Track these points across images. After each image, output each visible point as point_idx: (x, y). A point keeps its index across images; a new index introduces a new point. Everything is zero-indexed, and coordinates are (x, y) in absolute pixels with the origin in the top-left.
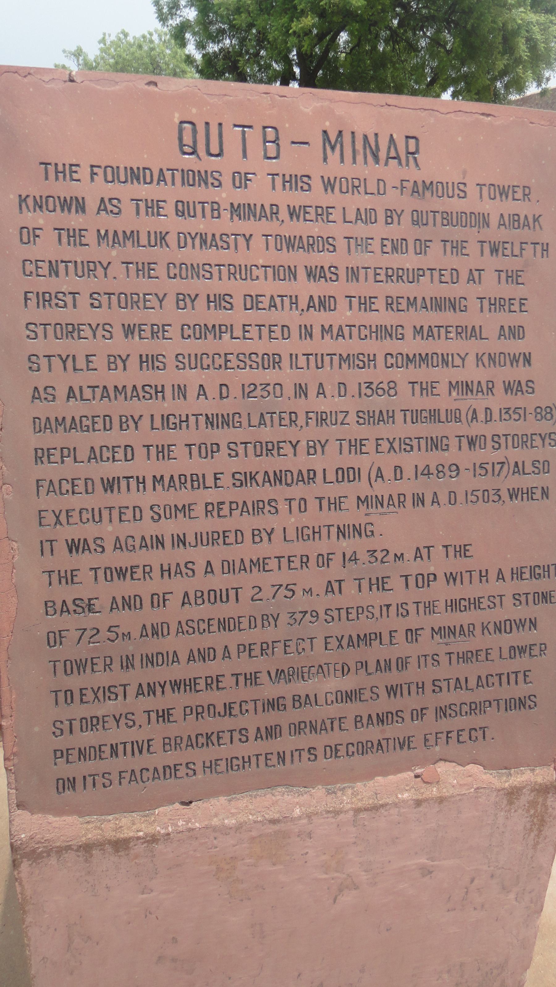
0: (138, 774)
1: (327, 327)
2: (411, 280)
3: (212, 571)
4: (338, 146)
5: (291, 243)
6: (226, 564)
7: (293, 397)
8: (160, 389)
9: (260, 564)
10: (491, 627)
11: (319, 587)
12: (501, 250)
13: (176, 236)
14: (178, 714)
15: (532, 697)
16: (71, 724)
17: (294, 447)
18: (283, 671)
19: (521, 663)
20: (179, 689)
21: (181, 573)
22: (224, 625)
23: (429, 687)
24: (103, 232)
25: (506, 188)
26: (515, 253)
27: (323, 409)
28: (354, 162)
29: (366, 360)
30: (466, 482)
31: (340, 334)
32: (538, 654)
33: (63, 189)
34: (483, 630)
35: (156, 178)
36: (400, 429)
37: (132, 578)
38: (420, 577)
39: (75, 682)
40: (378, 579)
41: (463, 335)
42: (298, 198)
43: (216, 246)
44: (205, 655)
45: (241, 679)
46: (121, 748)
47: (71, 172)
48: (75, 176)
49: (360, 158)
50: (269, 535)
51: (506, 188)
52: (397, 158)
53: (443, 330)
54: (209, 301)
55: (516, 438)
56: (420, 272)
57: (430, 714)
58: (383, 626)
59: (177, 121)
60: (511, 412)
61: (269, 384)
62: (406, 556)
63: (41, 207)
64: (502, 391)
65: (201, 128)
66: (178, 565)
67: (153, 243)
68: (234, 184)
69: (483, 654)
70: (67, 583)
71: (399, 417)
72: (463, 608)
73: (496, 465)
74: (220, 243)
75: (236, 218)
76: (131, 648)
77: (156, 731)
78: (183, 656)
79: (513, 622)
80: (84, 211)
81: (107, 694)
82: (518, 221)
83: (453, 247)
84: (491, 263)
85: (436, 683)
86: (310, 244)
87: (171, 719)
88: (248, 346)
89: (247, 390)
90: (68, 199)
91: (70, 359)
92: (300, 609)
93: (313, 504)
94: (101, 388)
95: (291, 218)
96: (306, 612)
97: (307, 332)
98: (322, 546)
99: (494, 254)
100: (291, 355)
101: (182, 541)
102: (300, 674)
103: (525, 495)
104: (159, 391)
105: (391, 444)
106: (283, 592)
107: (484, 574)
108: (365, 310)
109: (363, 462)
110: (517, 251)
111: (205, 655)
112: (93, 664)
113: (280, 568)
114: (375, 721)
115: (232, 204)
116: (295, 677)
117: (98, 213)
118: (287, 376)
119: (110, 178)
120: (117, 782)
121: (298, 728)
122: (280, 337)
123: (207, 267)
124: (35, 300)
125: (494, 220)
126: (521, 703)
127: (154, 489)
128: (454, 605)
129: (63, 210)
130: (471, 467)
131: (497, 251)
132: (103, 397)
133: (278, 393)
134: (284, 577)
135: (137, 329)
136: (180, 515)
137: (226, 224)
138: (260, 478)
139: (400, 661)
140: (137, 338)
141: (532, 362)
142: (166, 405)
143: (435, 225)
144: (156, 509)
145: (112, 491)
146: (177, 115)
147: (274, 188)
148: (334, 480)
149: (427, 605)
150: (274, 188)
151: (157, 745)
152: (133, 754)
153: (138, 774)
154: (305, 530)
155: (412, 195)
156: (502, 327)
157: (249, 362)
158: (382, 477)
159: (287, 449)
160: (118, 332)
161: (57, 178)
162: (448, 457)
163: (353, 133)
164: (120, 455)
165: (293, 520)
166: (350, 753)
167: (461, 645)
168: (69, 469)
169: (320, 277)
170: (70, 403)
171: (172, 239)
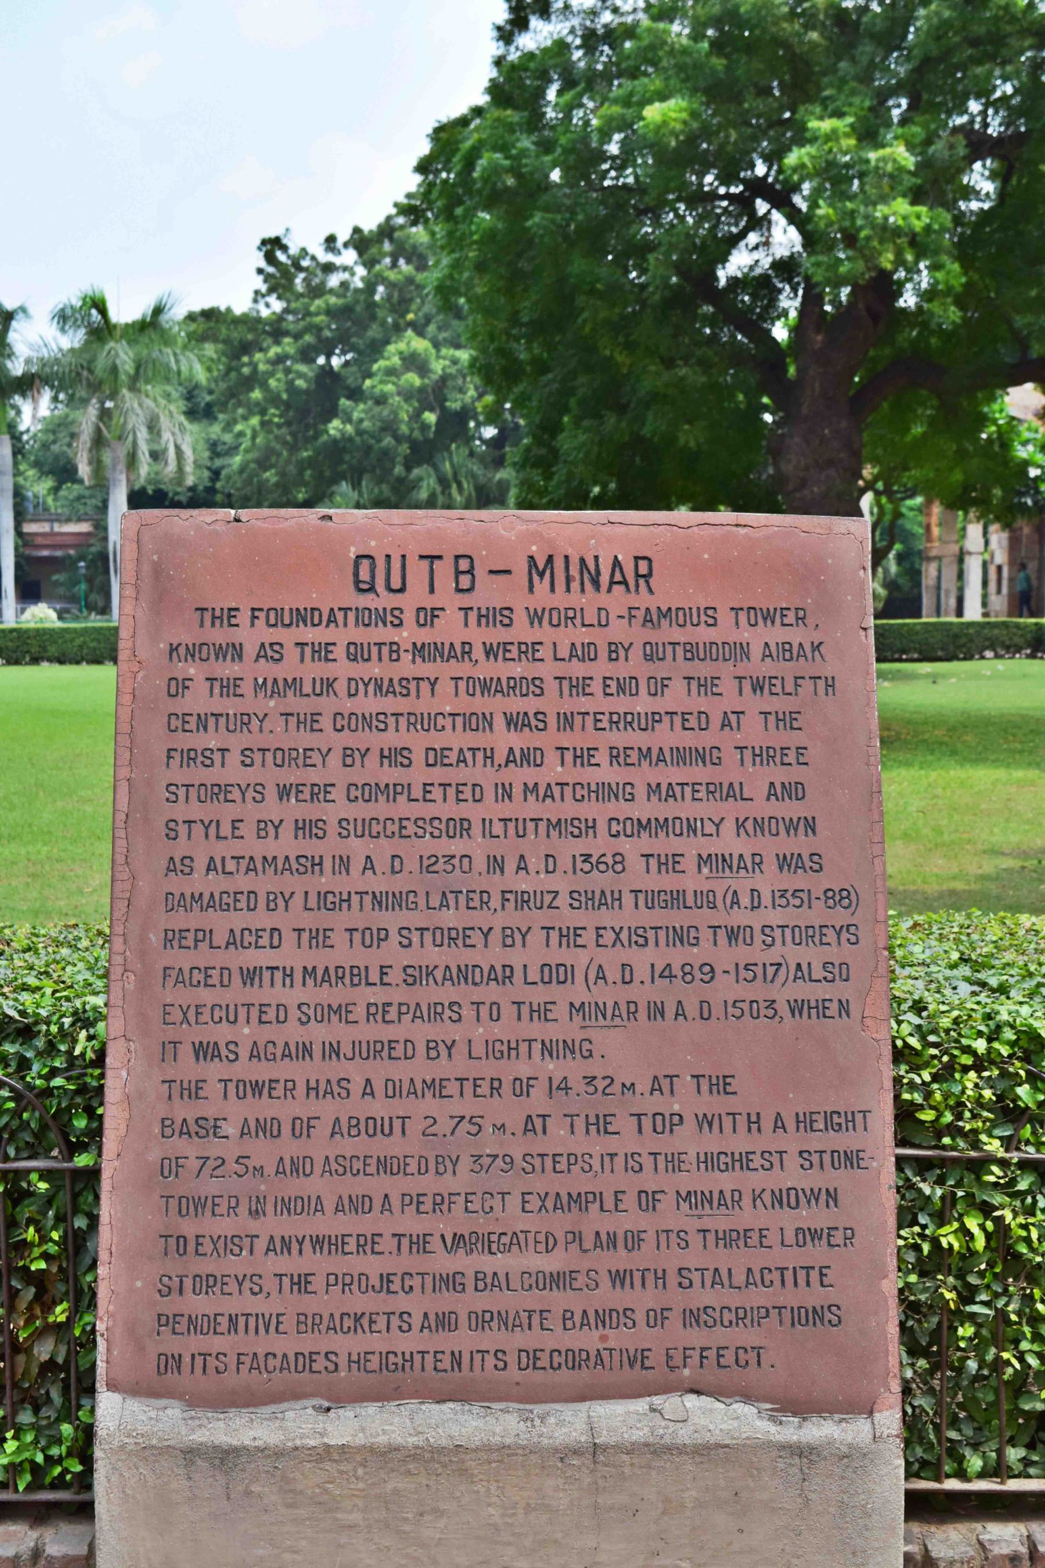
0: (261, 1359)
1: (531, 787)
2: (643, 726)
3: (372, 1094)
4: (548, 572)
5: (485, 686)
6: (390, 1083)
7: (484, 873)
8: (317, 861)
9: (436, 1087)
10: (767, 1197)
11: (515, 1122)
12: (767, 686)
13: (346, 683)
14: (318, 1283)
15: (834, 1309)
16: (181, 1281)
17: (486, 936)
18: (462, 1236)
19: (816, 1254)
20: (321, 1248)
21: (332, 1093)
22: (384, 1165)
23: (673, 1279)
24: (260, 681)
25: (772, 611)
26: (788, 690)
27: (524, 887)
28: (568, 590)
29: (583, 826)
30: (726, 989)
31: (549, 795)
32: (842, 1243)
33: (219, 635)
34: (754, 1201)
35: (325, 618)
36: (628, 916)
37: (270, 1097)
38: (659, 1118)
39: (189, 1228)
40: (597, 1116)
41: (717, 795)
42: (496, 635)
43: (394, 692)
44: (359, 1204)
45: (405, 1242)
46: (242, 1320)
47: (230, 617)
48: (233, 621)
49: (575, 585)
50: (449, 1048)
51: (772, 611)
52: (624, 582)
53: (688, 790)
54: (382, 757)
55: (797, 930)
56: (655, 718)
57: (675, 1320)
58: (606, 1184)
59: (353, 556)
60: (788, 895)
61: (453, 857)
62: (639, 1088)
63: (193, 656)
64: (775, 867)
65: (381, 564)
66: (328, 1081)
67: (318, 691)
68: (418, 622)
69: (755, 1236)
70: (190, 1097)
71: (628, 899)
72: (723, 1167)
73: (768, 968)
74: (398, 689)
75: (418, 660)
76: (263, 1187)
77: (291, 1304)
78: (329, 1205)
79: (800, 1193)
80: (240, 657)
81: (230, 1246)
82: (790, 651)
83: (700, 685)
84: (753, 703)
85: (684, 1273)
86: (514, 686)
87: (310, 1288)
88: (428, 810)
89: (426, 863)
90: (224, 646)
91: (214, 824)
92: (488, 1151)
93: (508, 1011)
94: (247, 860)
95: (488, 657)
96: (496, 1156)
97: (506, 792)
98: (523, 1069)
99: (758, 692)
100: (484, 820)
101: (333, 1051)
102: (486, 1243)
103: (814, 1011)
104: (318, 863)
105: (618, 934)
106: (465, 1125)
107: (754, 1118)
108: (582, 765)
109: (580, 959)
110: (789, 688)
111: (359, 1204)
112: (214, 1205)
113: (462, 1094)
114: (592, 1321)
115: (414, 644)
116: (479, 1245)
117: (256, 660)
118: (477, 847)
119: (272, 621)
120: (234, 1367)
121: (481, 1321)
122: (471, 799)
123: (382, 717)
124: (178, 759)
125: (756, 651)
126: (816, 1315)
127: (304, 984)
128: (709, 1161)
129: (217, 658)
130: (732, 968)
131: (762, 689)
132: (248, 870)
133: (466, 868)
134: (467, 1106)
135: (294, 791)
136: (335, 1018)
137: (407, 667)
138: (439, 974)
139: (629, 1234)
140: (293, 800)
141: (817, 830)
142: (323, 880)
143: (674, 659)
144: (304, 1008)
145: (252, 985)
146: (353, 549)
147: (466, 625)
148: (537, 979)
149: (670, 1158)
150: (466, 625)
151: (288, 1323)
152: (257, 1332)
153: (261, 1359)
154: (498, 1044)
155: (644, 625)
156: (772, 784)
157: (429, 829)
158: (604, 978)
159: (476, 938)
160: (271, 793)
161: (213, 624)
162: (695, 955)
163: (566, 557)
164: (265, 941)
165: (481, 1030)
166: (556, 1365)
167: (719, 1221)
168: (203, 956)
169: (523, 725)
170: (210, 877)
171: (341, 686)
